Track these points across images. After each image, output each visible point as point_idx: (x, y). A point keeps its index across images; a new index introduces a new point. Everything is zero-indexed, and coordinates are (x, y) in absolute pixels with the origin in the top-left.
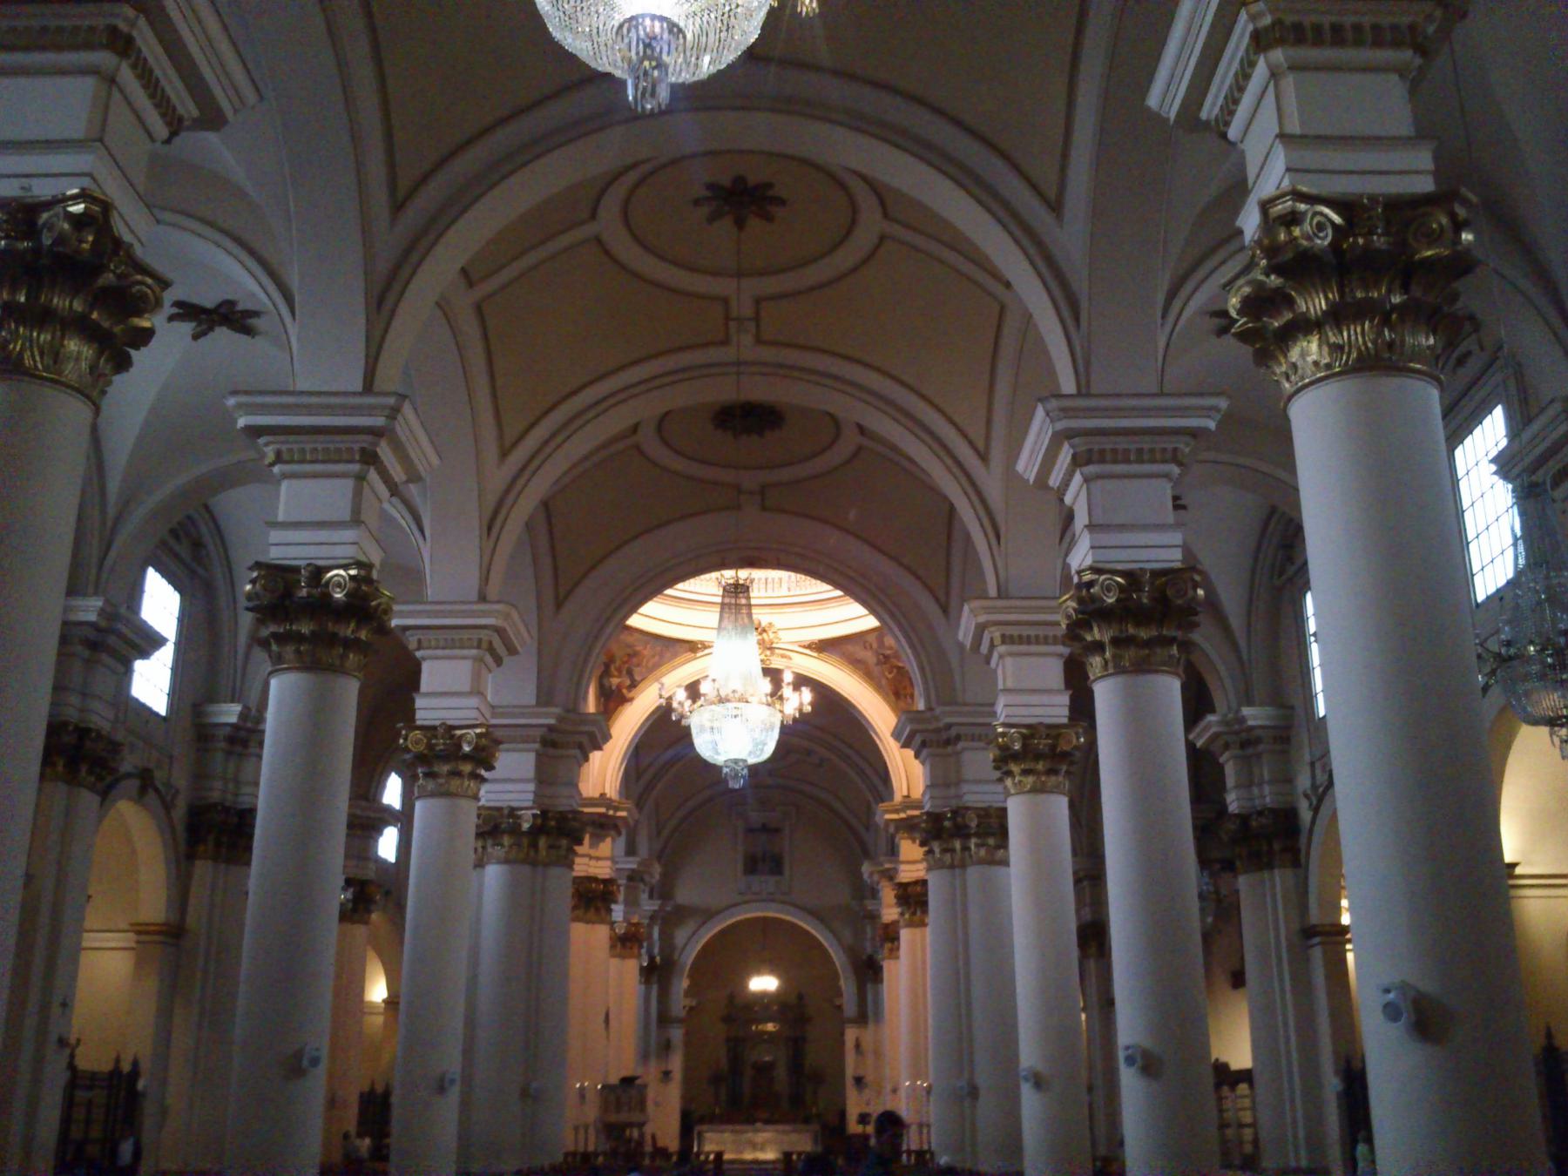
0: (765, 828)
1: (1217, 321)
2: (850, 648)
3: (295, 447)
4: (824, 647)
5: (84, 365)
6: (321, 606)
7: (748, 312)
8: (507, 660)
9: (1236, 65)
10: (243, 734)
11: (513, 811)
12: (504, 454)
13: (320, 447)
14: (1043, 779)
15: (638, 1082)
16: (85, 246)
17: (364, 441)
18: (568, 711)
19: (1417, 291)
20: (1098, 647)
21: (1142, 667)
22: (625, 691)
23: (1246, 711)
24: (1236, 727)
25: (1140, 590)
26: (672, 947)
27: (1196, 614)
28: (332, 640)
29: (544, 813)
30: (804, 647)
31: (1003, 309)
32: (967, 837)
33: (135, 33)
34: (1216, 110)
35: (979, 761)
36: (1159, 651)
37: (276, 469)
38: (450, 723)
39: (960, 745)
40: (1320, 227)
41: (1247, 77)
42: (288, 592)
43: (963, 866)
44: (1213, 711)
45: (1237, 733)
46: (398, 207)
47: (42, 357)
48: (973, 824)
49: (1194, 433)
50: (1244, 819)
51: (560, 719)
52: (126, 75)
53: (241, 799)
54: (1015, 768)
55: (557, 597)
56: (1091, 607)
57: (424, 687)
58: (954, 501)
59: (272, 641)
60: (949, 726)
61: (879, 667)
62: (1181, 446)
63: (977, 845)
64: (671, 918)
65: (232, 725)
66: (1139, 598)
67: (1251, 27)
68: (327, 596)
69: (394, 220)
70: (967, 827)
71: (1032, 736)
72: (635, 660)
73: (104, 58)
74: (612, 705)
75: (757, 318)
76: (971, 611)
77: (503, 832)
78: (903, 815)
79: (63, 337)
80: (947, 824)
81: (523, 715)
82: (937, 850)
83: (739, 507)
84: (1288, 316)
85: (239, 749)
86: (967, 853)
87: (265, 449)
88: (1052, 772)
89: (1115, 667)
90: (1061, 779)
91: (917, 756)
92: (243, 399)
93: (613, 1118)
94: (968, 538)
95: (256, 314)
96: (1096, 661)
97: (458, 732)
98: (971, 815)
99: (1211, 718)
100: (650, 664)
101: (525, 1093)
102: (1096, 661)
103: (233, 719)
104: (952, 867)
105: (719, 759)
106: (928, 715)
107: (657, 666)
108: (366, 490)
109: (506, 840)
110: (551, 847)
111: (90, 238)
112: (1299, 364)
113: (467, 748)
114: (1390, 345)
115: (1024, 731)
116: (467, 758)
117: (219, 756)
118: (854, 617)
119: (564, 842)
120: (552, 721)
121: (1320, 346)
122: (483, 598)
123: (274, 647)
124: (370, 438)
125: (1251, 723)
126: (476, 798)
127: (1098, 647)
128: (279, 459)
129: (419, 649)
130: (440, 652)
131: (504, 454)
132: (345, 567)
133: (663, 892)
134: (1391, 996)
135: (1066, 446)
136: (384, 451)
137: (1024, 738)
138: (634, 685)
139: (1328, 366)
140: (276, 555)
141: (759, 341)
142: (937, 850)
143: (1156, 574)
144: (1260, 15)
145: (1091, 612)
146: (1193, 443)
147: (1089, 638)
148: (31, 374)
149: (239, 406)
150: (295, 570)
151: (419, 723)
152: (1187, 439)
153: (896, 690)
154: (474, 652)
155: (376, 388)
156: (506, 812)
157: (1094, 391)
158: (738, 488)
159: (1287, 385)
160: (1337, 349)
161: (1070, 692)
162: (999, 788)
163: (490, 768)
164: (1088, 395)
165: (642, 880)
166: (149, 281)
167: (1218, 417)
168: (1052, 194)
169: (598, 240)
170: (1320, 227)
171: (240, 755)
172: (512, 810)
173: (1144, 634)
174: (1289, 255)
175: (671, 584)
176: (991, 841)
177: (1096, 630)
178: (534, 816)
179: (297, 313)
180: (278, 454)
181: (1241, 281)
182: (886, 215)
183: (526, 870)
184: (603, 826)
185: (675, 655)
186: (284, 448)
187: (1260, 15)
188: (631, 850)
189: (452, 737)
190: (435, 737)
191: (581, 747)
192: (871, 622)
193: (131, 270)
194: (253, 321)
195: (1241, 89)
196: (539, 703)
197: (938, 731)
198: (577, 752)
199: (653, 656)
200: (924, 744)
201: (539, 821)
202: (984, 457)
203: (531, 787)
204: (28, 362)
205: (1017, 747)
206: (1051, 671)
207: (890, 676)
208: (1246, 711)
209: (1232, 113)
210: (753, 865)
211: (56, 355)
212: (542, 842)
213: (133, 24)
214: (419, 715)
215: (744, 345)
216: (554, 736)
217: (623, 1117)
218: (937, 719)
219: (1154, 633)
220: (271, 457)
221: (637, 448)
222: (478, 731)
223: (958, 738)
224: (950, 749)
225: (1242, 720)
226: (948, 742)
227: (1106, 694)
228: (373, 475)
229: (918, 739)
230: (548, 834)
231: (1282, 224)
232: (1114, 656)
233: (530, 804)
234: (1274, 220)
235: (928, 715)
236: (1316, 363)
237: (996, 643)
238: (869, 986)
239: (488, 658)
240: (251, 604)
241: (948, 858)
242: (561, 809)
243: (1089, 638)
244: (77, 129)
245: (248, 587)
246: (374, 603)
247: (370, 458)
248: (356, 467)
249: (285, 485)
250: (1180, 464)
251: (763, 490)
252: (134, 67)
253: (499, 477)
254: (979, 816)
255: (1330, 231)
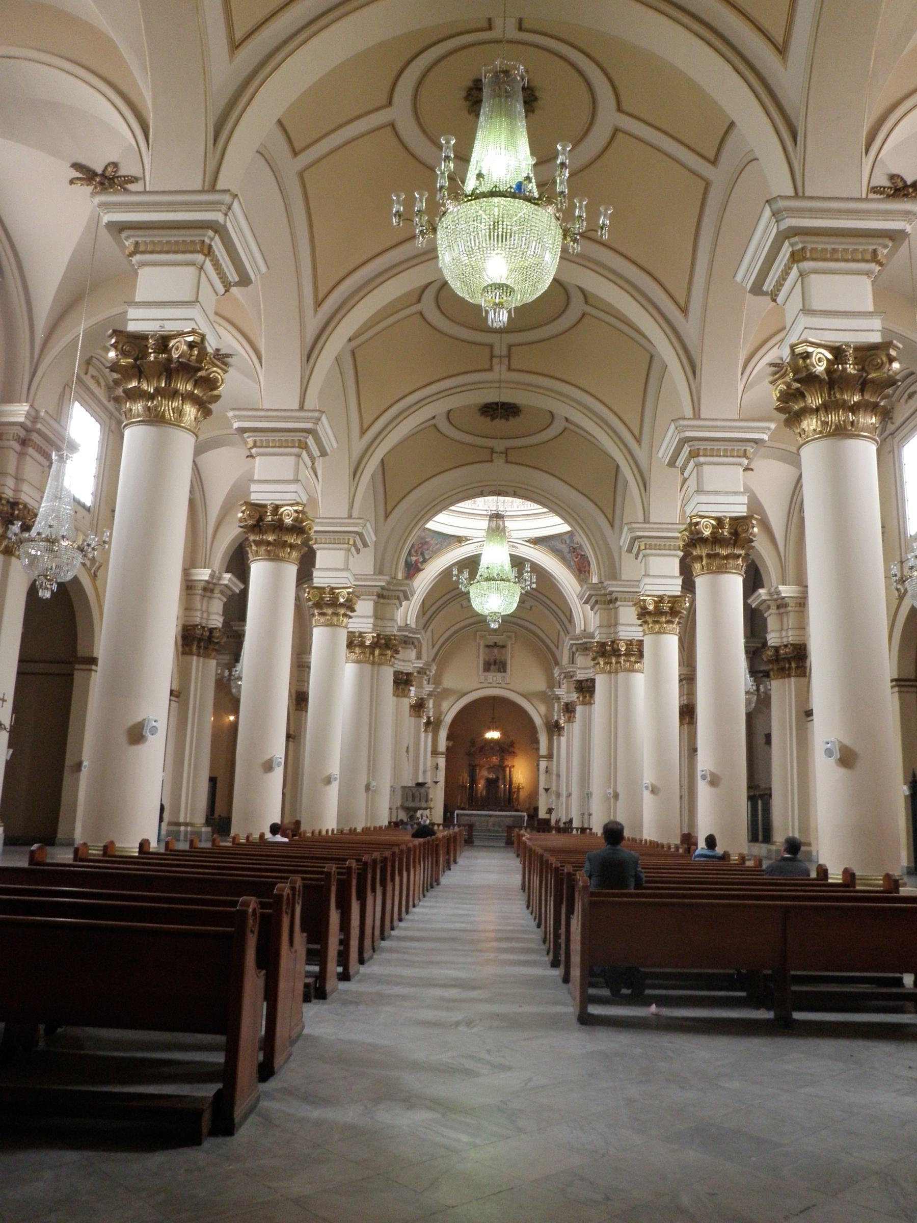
0: (495, 645)
1: (774, 369)
2: (553, 543)
3: (264, 439)
4: (537, 541)
5: (193, 417)
6: (279, 526)
7: (504, 352)
8: (363, 550)
9: (782, 267)
10: (211, 585)
11: (361, 634)
12: (363, 432)
13: (277, 439)
14: (665, 626)
15: (426, 785)
16: (194, 358)
17: (297, 437)
18: (392, 578)
19: (867, 397)
20: (700, 558)
21: (722, 570)
22: (419, 564)
23: (781, 588)
24: (775, 597)
25: (722, 528)
26: (441, 714)
27: (753, 541)
28: (284, 544)
29: (378, 635)
30: (526, 541)
31: (652, 357)
32: (620, 656)
33: (213, 244)
34: (771, 287)
35: (628, 614)
36: (731, 561)
37: (253, 451)
38: (333, 585)
39: (618, 603)
40: (820, 360)
41: (788, 274)
42: (261, 519)
43: (616, 672)
44: (762, 587)
45: (776, 600)
46: (318, 304)
47: (173, 413)
48: (623, 649)
49: (756, 441)
50: (777, 649)
51: (389, 583)
52: (208, 265)
53: (210, 622)
54: (650, 620)
55: (386, 513)
56: (696, 537)
57: (317, 566)
58: (620, 465)
59: (253, 544)
60: (611, 593)
61: (570, 555)
62: (748, 448)
63: (624, 661)
64: (440, 695)
65: (206, 581)
66: (723, 532)
67: (791, 250)
68: (281, 521)
69: (316, 311)
70: (619, 650)
71: (660, 602)
72: (426, 547)
73: (200, 257)
74: (412, 572)
75: (509, 356)
76: (629, 529)
77: (355, 645)
78: (580, 642)
79: (183, 404)
80: (608, 648)
81: (366, 580)
82: (602, 663)
83: (492, 461)
84: (802, 405)
85: (209, 594)
86: (619, 665)
87: (248, 440)
88: (668, 622)
89: (707, 570)
90: (674, 626)
91: (592, 609)
92: (237, 413)
93: (411, 805)
94: (626, 483)
95: (228, 356)
96: (697, 566)
97: (337, 591)
98: (622, 644)
99: (761, 591)
100: (434, 549)
101: (368, 788)
102: (697, 566)
103: (207, 578)
104: (610, 672)
105: (486, 612)
106: (600, 585)
107: (439, 550)
108: (301, 461)
109: (357, 650)
110: (380, 654)
111: (196, 352)
112: (806, 429)
113: (342, 600)
114: (852, 423)
115: (656, 599)
116: (342, 605)
117: (198, 598)
118: (555, 525)
119: (389, 653)
120: (383, 584)
121: (817, 421)
122: (350, 517)
123: (254, 548)
124: (305, 434)
125: (783, 595)
126: (346, 627)
127: (700, 558)
128: (255, 446)
129: (315, 544)
130: (326, 546)
131: (363, 432)
132: (291, 505)
133: (437, 680)
134: (829, 745)
135: (686, 446)
136: (310, 441)
137: (655, 602)
138: (425, 561)
139: (821, 432)
140: (255, 498)
141: (509, 369)
142: (602, 663)
143: (732, 519)
144: (796, 243)
145: (694, 540)
146: (755, 446)
147: (695, 553)
148: (169, 423)
149: (235, 416)
150: (265, 506)
151: (315, 585)
152: (752, 444)
153: (581, 568)
154: (346, 546)
155: (305, 408)
156: (357, 634)
157: (702, 416)
158: (492, 451)
159: (800, 439)
160: (825, 423)
161: (683, 577)
162: (641, 629)
163: (353, 610)
164: (699, 418)
165: (425, 673)
166: (219, 371)
167: (769, 433)
168: (682, 303)
169: (421, 313)
170: (820, 360)
171: (210, 598)
172: (361, 633)
173: (724, 552)
174: (804, 374)
175: (453, 504)
176: (633, 659)
177: (698, 548)
178: (373, 637)
179: (263, 362)
180: (255, 442)
181: (780, 382)
182: (586, 302)
183: (368, 667)
184: (407, 642)
185: (449, 544)
186: (258, 439)
187: (796, 243)
188: (419, 657)
189: (333, 593)
190: (324, 593)
191: (398, 598)
192: (566, 528)
193: (211, 366)
194: (229, 360)
195: (785, 280)
196: (374, 574)
197: (605, 595)
198: (397, 602)
199: (437, 544)
200: (596, 602)
201: (376, 640)
202: (638, 441)
203: (371, 620)
204: (167, 416)
205: (651, 608)
206: (672, 565)
207: (576, 560)
208: (781, 588)
209: (779, 290)
210: (487, 667)
211: (180, 413)
212: (377, 652)
213: (212, 239)
214: (315, 580)
215: (500, 371)
216: (385, 593)
217: (416, 805)
218: (605, 588)
219: (729, 551)
220: (251, 444)
221: (435, 426)
222: (348, 590)
223: (616, 599)
224: (611, 606)
225: (778, 593)
226: (610, 602)
227: (701, 583)
228: (304, 454)
229: (593, 600)
230: (380, 647)
231: (801, 358)
232: (707, 564)
233: (370, 630)
234: (797, 355)
235: (600, 585)
236: (815, 430)
237: (641, 548)
238: (555, 737)
239: (353, 550)
240: (242, 524)
241: (608, 668)
242: (387, 633)
243: (695, 553)
244: (188, 296)
245: (240, 515)
246: (304, 524)
247: (304, 446)
248: (296, 450)
249: (258, 459)
250: (748, 458)
251: (506, 452)
252: (211, 261)
253: (359, 445)
254: (627, 644)
255: (825, 362)
